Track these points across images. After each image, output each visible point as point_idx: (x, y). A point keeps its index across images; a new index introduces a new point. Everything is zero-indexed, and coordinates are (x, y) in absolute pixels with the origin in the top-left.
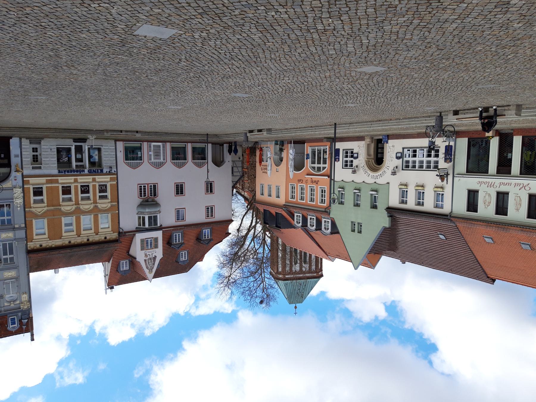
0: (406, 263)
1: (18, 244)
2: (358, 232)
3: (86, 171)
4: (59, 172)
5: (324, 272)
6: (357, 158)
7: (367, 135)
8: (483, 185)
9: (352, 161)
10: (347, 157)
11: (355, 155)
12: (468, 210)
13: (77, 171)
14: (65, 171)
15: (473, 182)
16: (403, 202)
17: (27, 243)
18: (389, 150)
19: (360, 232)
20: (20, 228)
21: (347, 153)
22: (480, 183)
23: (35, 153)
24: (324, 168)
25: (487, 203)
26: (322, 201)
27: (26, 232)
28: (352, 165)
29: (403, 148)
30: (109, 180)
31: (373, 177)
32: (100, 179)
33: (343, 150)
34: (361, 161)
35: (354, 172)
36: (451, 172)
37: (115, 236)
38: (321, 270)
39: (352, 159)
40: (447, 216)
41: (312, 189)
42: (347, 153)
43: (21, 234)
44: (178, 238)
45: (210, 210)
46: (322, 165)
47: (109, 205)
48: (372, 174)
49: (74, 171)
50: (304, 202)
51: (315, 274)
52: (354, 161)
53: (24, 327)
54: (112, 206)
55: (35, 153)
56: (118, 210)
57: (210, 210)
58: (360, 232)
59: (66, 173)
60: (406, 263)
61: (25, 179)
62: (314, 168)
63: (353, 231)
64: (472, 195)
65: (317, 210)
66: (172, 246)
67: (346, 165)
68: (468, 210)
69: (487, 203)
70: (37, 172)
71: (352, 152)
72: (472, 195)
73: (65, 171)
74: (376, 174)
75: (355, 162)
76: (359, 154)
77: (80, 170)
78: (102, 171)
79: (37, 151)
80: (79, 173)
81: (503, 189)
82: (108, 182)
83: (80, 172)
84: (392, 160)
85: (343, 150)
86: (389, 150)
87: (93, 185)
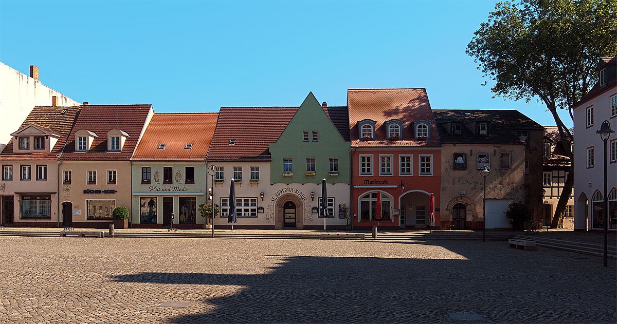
12: (193, 168)
15: (190, 191)
18: (272, 216)
22: (184, 190)
24: (367, 196)
46: (371, 200)
62: (384, 197)
63: (315, 133)
68: (193, 168)
81: (167, 186)
84: (269, 206)
86: (272, 216)
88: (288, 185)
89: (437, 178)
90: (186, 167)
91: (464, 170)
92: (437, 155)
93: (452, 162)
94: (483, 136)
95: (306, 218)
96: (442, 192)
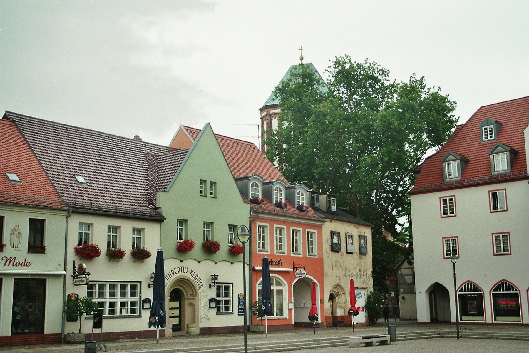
0: (133, 138)
2: (205, 181)
5: (258, 116)
6: (211, 301)
7: (195, 336)
8: (22, 261)
9: (218, 295)
10: (227, 302)
11: (213, 304)
12: (43, 221)
16: (140, 231)
19: (203, 182)
21: (227, 309)
22: (26, 264)
25: (16, 233)
26: (262, 229)
28: (219, 288)
29: (140, 316)
31: (185, 270)
33: (232, 313)
34: (205, 294)
35: (214, 278)
36: (69, 280)
38: (262, 118)
39: (218, 299)
40: (74, 212)
41: (281, 248)
42: (227, 309)
44: (501, 163)
45: (449, 209)
48: (187, 275)
50: (292, 228)
51: (272, 112)
52: (214, 295)
57: (449, 209)
58: (203, 182)
60: (133, 138)
63: (213, 184)
64: (37, 246)
65: (270, 214)
66: (509, 149)
67: (227, 288)
68: (43, 221)
69: (16, 233)
71: (219, 309)
72: (37, 246)
74: (181, 274)
75: (213, 293)
76: (208, 308)
85: (232, 313)
88: (181, 261)
89: (320, 261)
90: (31, 220)
91: (338, 252)
92: (319, 228)
93: (330, 241)
94: (333, 213)
95: (203, 316)
96: (325, 279)
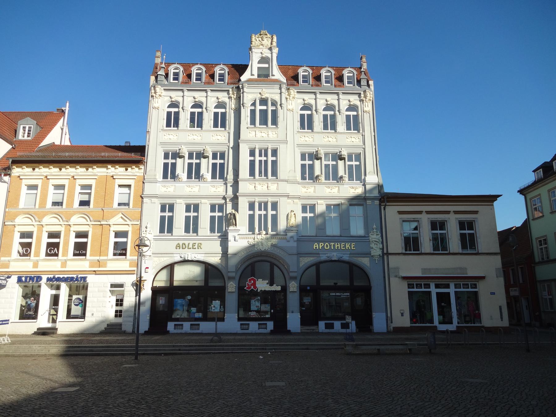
1: (155, 175)
3: (44, 278)
4: (85, 278)
13: (59, 279)
14: (77, 280)
17: (144, 176)
20: (151, 197)
23: (119, 308)
27: (143, 190)
30: (12, 263)
32: (26, 266)
37: (16, 171)
43: (149, 189)
47: (19, 220)
49: (65, 280)
53: (163, 66)
54: (13, 220)
55: (119, 308)
56: (5, 212)
59: (75, 276)
61: (135, 269)
70: (118, 279)
73: (77, 280)
77: (55, 282)
78: (19, 280)
79: (116, 311)
80: (57, 276)
82: (16, 260)
83: (54, 277)
87: (38, 256)
